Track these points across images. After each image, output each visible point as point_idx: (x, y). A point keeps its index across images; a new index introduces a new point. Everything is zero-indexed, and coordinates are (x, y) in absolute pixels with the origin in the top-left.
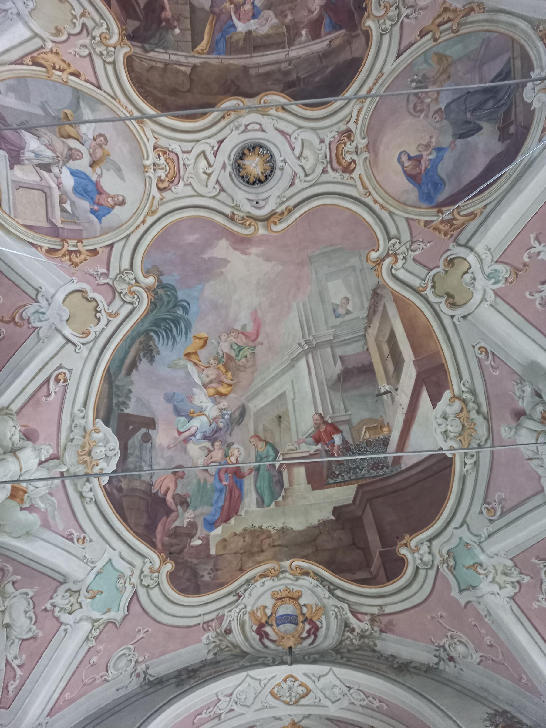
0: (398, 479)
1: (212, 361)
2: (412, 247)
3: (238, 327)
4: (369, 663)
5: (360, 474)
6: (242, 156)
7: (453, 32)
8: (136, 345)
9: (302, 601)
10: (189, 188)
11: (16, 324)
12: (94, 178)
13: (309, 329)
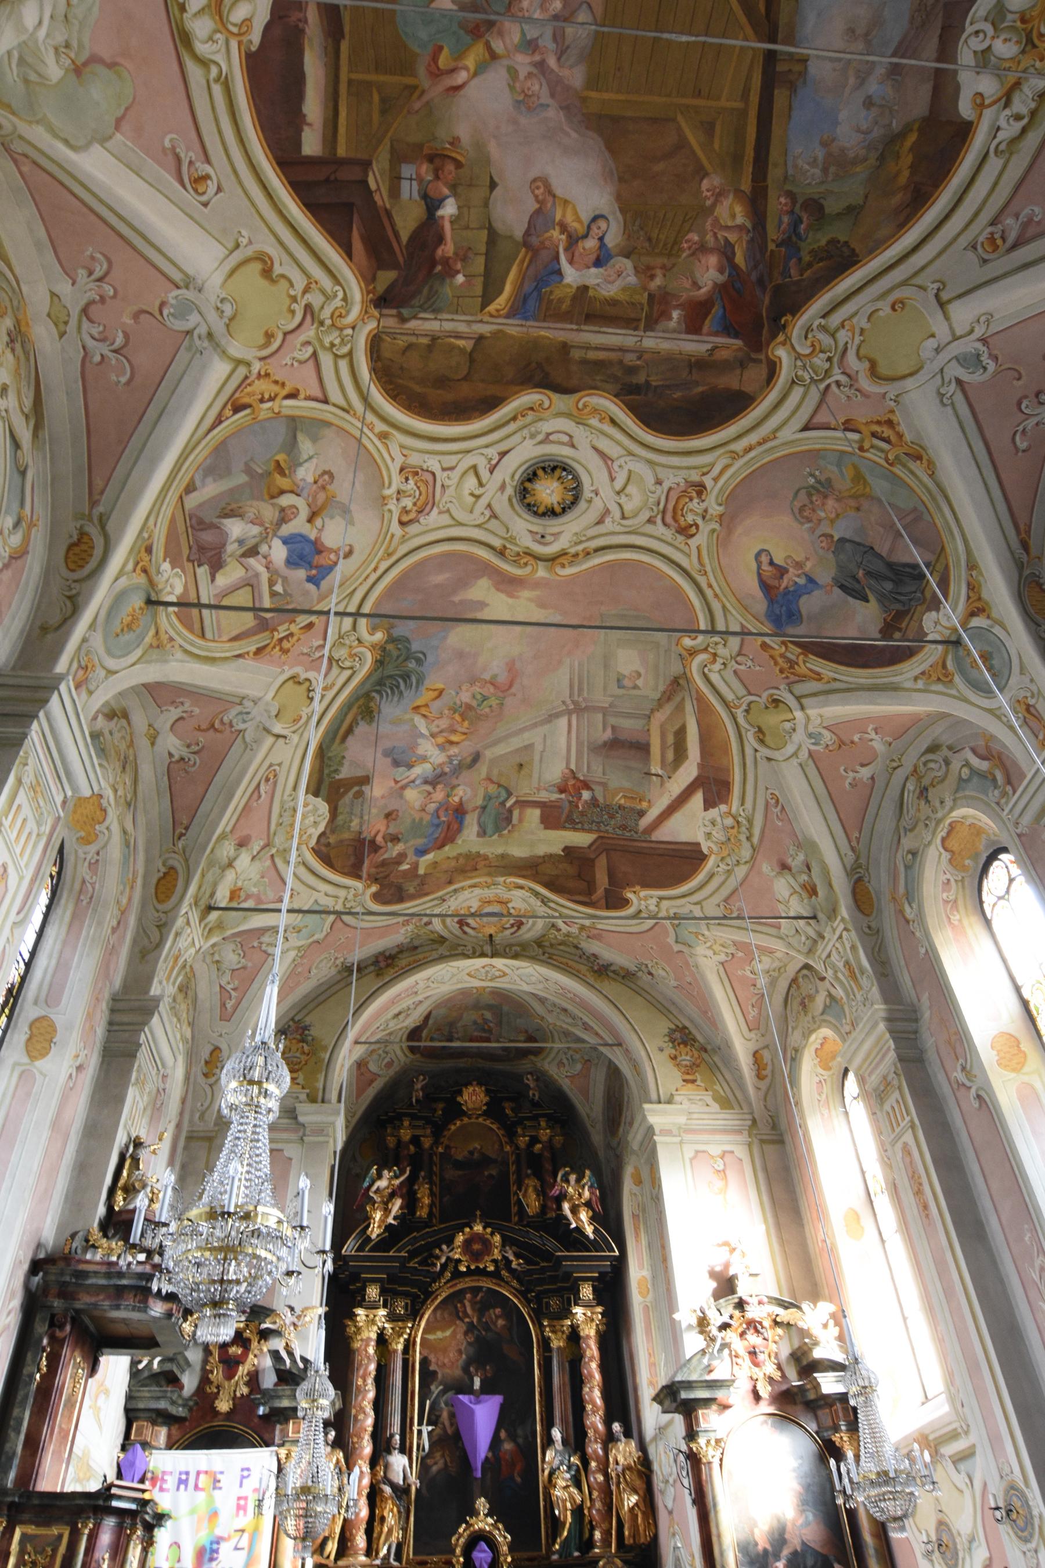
0: (644, 845)
1: (446, 712)
2: (739, 659)
3: (487, 676)
4: (570, 963)
5: (603, 827)
6: (532, 477)
7: (887, 460)
8: (354, 710)
9: (510, 905)
10: (446, 516)
11: (216, 730)
12: (313, 537)
13: (580, 690)
